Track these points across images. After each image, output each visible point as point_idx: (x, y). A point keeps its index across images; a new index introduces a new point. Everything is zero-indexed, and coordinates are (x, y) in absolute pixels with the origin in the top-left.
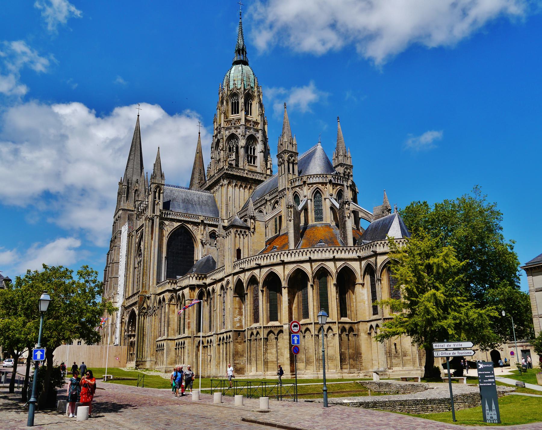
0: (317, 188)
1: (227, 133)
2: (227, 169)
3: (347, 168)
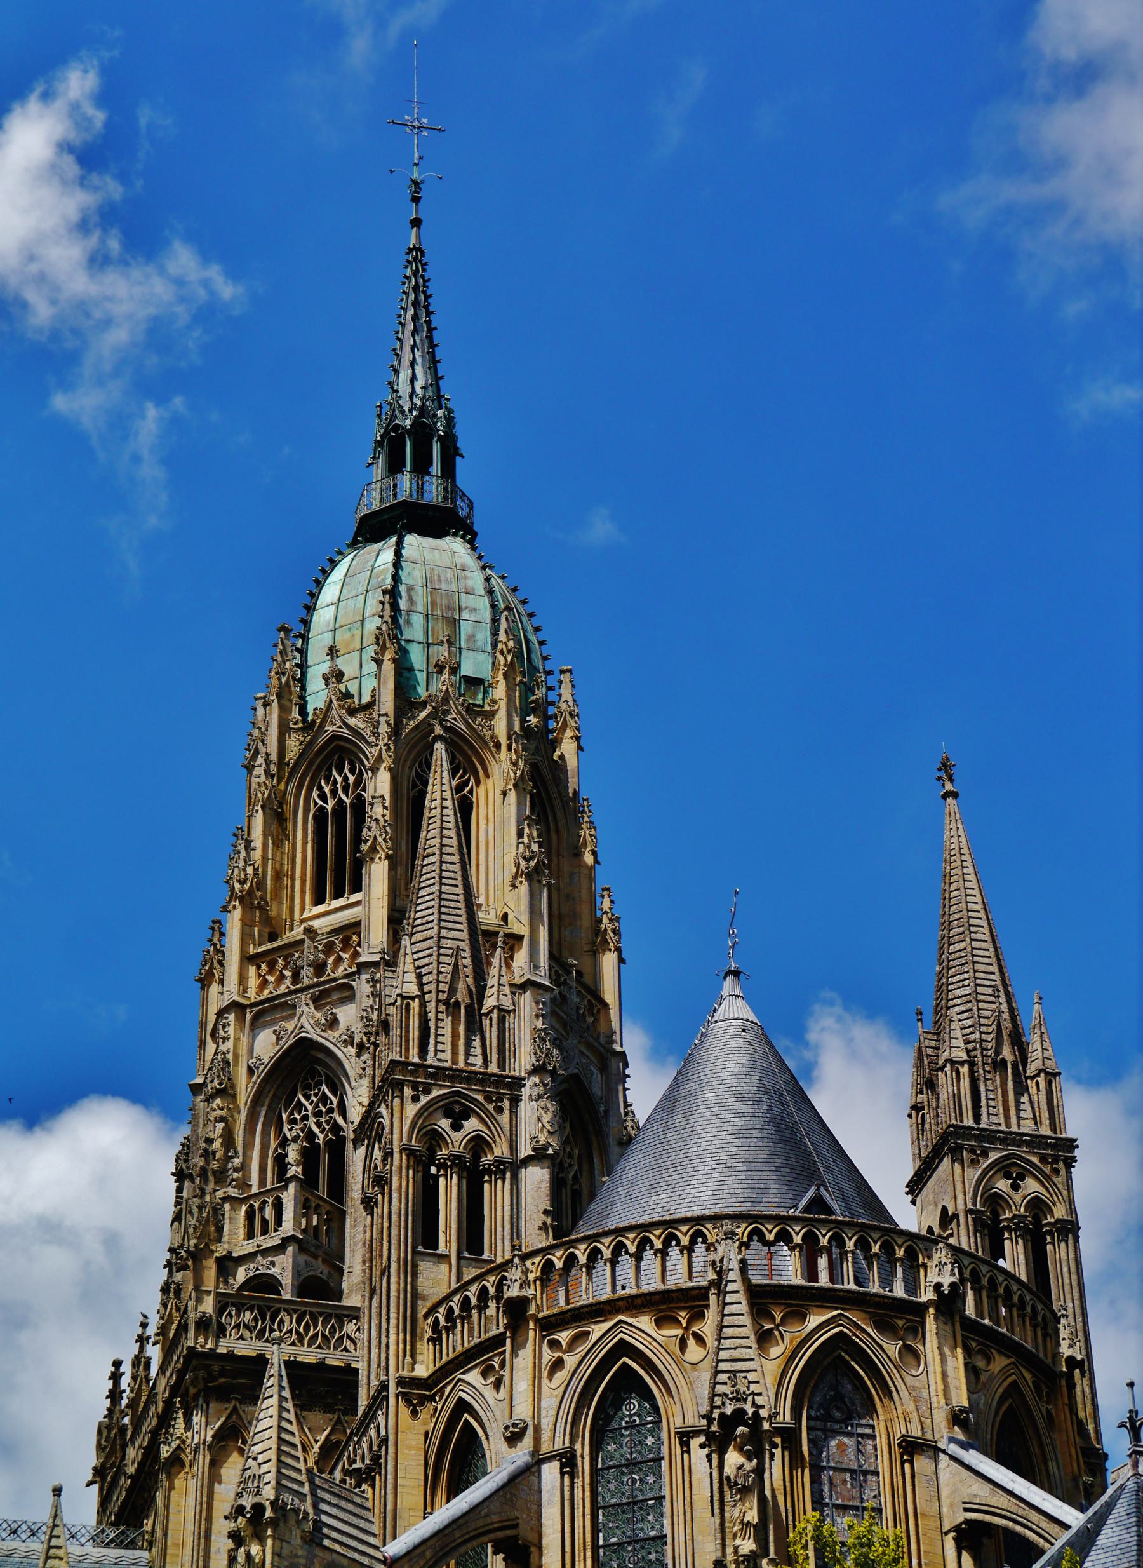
0: (623, 1348)
1: (267, 1045)
2: (203, 1325)
3: (1013, 1171)
